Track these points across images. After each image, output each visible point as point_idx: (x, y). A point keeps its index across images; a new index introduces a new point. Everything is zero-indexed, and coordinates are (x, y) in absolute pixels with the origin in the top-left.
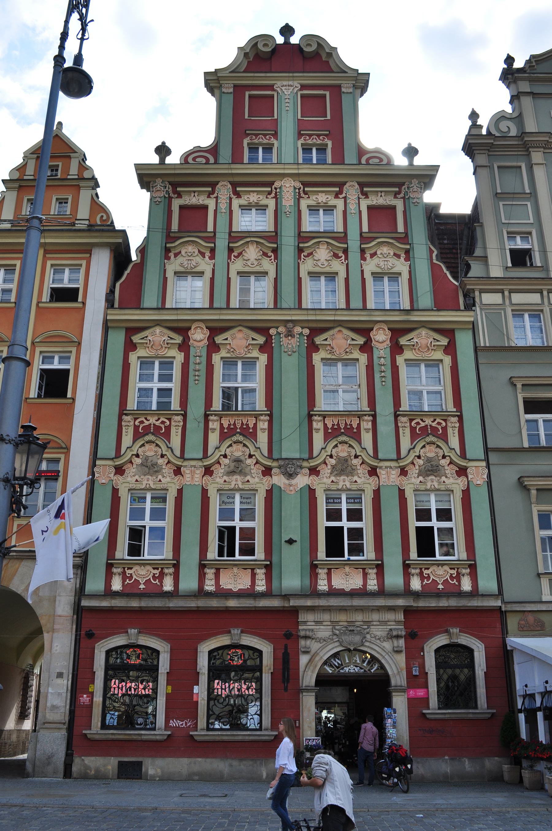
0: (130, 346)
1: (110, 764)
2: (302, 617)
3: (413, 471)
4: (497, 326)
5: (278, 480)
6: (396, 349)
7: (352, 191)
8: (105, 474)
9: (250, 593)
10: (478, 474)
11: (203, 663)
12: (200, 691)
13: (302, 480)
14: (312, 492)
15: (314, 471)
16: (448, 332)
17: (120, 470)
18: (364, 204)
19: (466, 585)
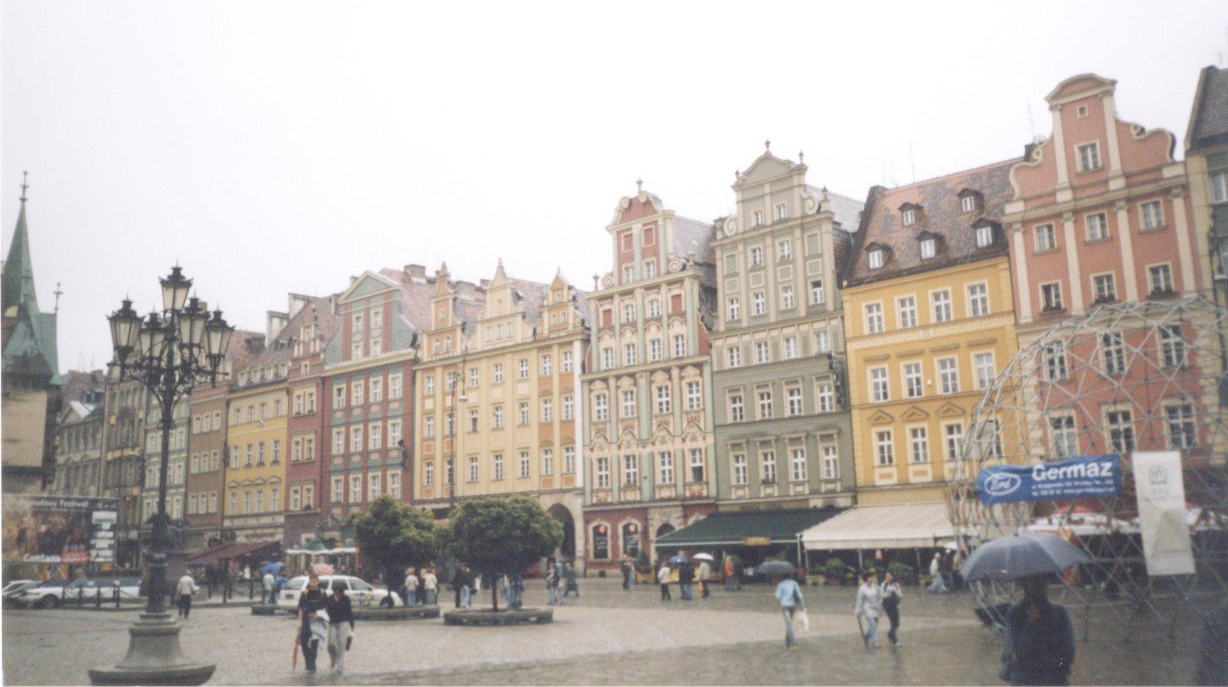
0: (591, 391)
1: (596, 571)
2: (651, 511)
3: (688, 440)
4: (720, 363)
5: (641, 449)
6: (681, 378)
7: (664, 288)
8: (588, 453)
9: (634, 502)
10: (710, 440)
11: (620, 531)
12: (621, 542)
13: (649, 449)
14: (652, 454)
15: (653, 443)
16: (699, 366)
17: (592, 450)
19: (705, 493)
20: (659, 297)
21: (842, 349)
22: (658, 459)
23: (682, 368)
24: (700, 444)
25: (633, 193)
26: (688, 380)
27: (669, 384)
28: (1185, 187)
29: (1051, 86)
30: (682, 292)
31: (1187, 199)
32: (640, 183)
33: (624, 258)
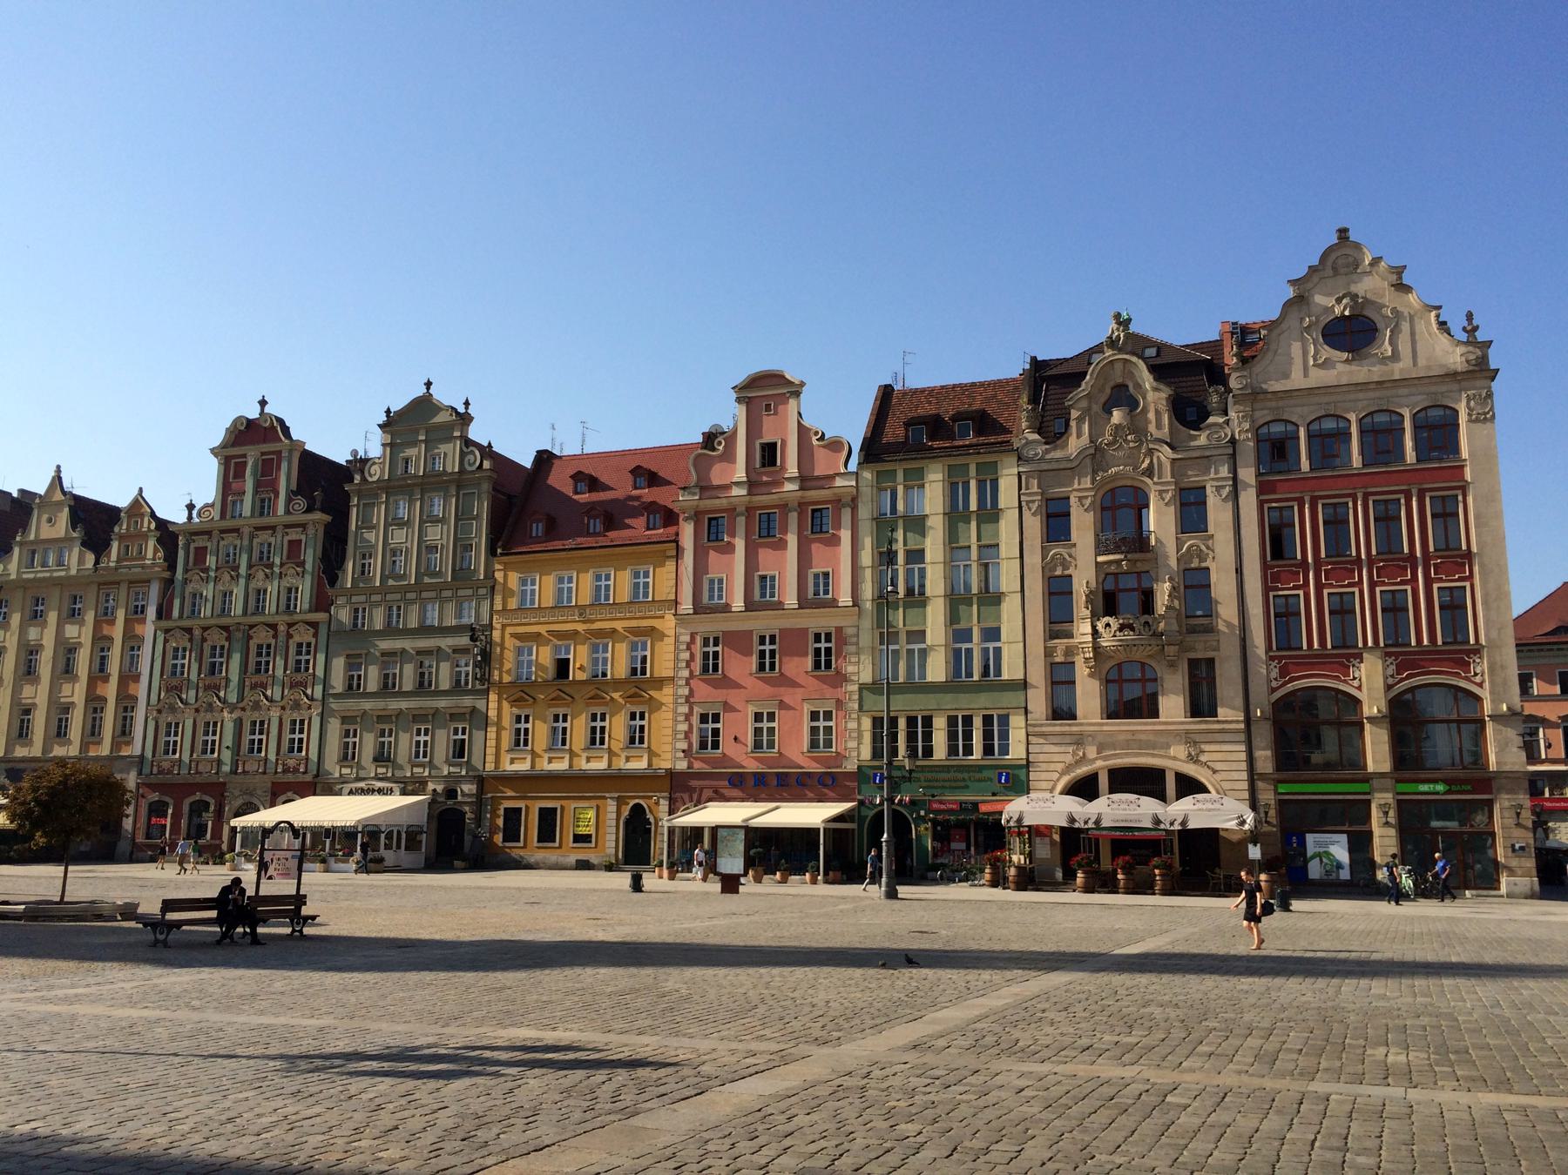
0: (166, 641)
14: (241, 720)
18: (286, 539)
20: (272, 540)
21: (486, 621)
22: (247, 727)
23: (290, 625)
24: (305, 714)
25: (253, 413)
26: (297, 638)
27: (273, 642)
28: (854, 499)
29: (740, 378)
30: (303, 538)
31: (854, 509)
32: (263, 403)
33: (228, 486)
